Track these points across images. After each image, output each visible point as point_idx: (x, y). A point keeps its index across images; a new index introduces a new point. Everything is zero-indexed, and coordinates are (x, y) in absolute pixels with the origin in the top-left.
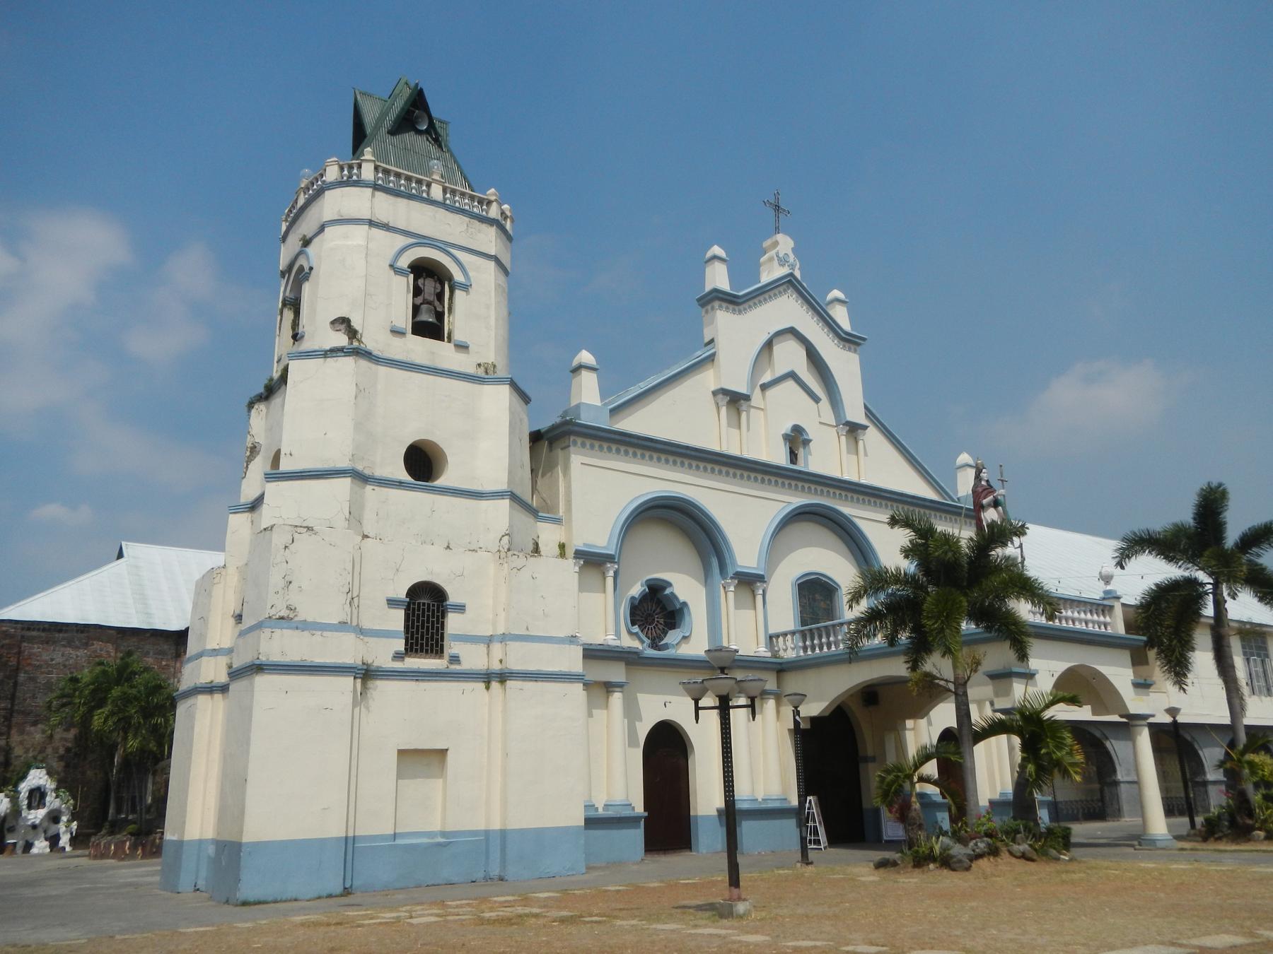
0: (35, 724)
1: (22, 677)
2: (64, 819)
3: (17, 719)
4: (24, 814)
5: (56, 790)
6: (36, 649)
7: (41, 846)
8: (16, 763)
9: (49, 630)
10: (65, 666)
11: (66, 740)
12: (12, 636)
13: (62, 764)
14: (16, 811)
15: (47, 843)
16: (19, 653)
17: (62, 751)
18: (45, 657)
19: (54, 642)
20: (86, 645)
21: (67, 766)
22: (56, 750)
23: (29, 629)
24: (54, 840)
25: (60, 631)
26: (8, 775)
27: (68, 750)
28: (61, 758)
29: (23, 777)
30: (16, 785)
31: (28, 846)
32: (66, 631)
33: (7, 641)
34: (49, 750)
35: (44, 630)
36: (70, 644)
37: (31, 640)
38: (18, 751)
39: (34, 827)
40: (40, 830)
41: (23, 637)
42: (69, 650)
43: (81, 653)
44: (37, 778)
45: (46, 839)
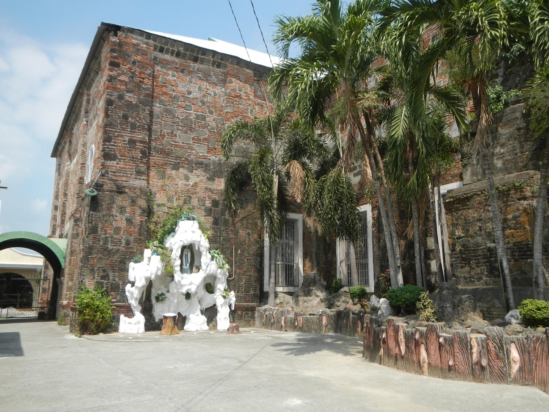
0: (176, 167)
1: (157, 108)
2: (221, 286)
3: (156, 158)
4: (177, 276)
5: (210, 249)
6: (171, 76)
7: (196, 322)
8: (160, 213)
9: (184, 56)
10: (203, 103)
11: (211, 190)
12: (144, 53)
13: (211, 219)
14: (168, 276)
15: (204, 319)
16: (154, 77)
17: (208, 204)
18: (182, 88)
19: (190, 73)
20: (224, 82)
21: (216, 222)
22: (202, 201)
23: (161, 50)
24: (211, 313)
25: (196, 60)
26: (152, 227)
27: (215, 203)
28: (209, 212)
29: (172, 231)
30: (162, 242)
31: (180, 321)
32: (202, 62)
33: (139, 58)
34: (195, 201)
35: (178, 55)
36: (206, 77)
37: (165, 64)
38: (160, 198)
39: (188, 296)
40: (194, 300)
41: (155, 58)
42: (205, 85)
43: (219, 90)
44: (189, 232)
45: (202, 312)
